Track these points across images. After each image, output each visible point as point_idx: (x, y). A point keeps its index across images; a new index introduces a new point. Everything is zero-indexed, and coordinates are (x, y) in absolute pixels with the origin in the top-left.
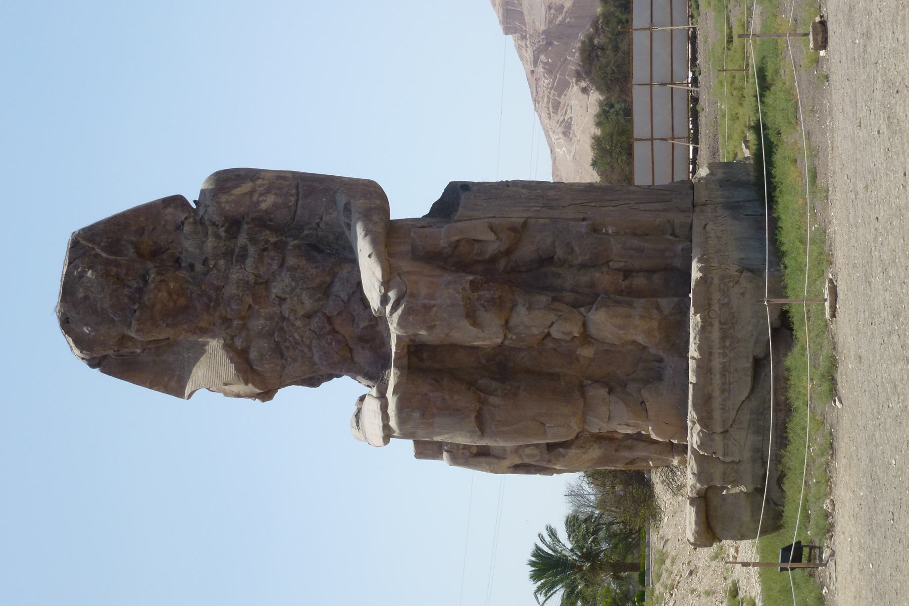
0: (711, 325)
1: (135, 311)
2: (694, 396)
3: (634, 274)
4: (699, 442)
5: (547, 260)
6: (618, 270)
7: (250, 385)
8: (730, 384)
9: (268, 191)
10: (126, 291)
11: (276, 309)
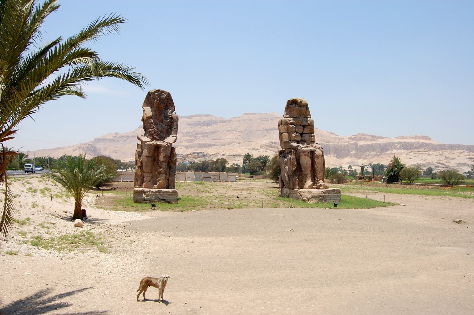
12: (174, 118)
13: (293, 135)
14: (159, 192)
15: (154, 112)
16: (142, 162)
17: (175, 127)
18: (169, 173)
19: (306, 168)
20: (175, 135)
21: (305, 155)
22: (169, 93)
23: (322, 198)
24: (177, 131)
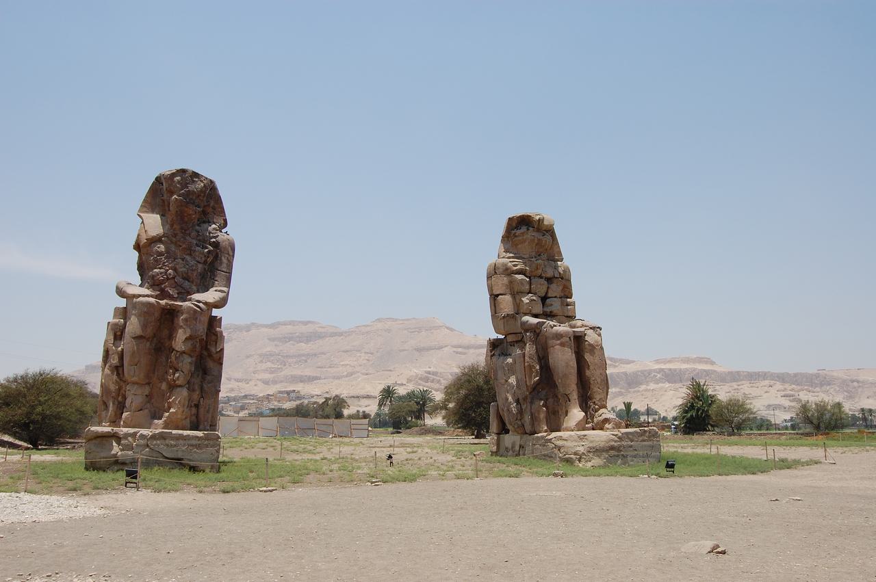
6: (199, 402)
9: (229, 261)
10: (194, 198)
11: (179, 257)
12: (223, 244)
13: (525, 300)
14: (162, 436)
15: (167, 227)
17: (224, 267)
18: (202, 389)
19: (565, 376)
20: (225, 289)
21: (562, 345)
22: (211, 182)
23: (615, 455)
24: (229, 280)
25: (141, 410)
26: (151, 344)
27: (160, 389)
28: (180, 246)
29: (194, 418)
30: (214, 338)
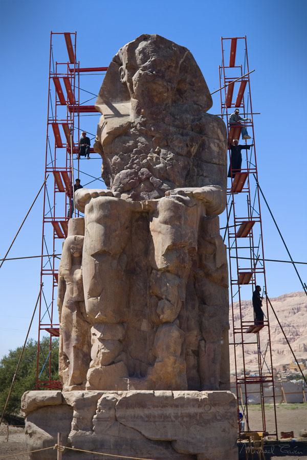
0: (199, 406)
1: (152, 73)
2: (144, 394)
3: (196, 357)
4: (109, 399)
5: (203, 301)
6: (199, 347)
7: (107, 135)
8: (155, 422)
16: (80, 284)
25: (113, 363)
26: (119, 262)
27: (139, 330)
28: (153, 137)
29: (194, 372)
30: (210, 249)
